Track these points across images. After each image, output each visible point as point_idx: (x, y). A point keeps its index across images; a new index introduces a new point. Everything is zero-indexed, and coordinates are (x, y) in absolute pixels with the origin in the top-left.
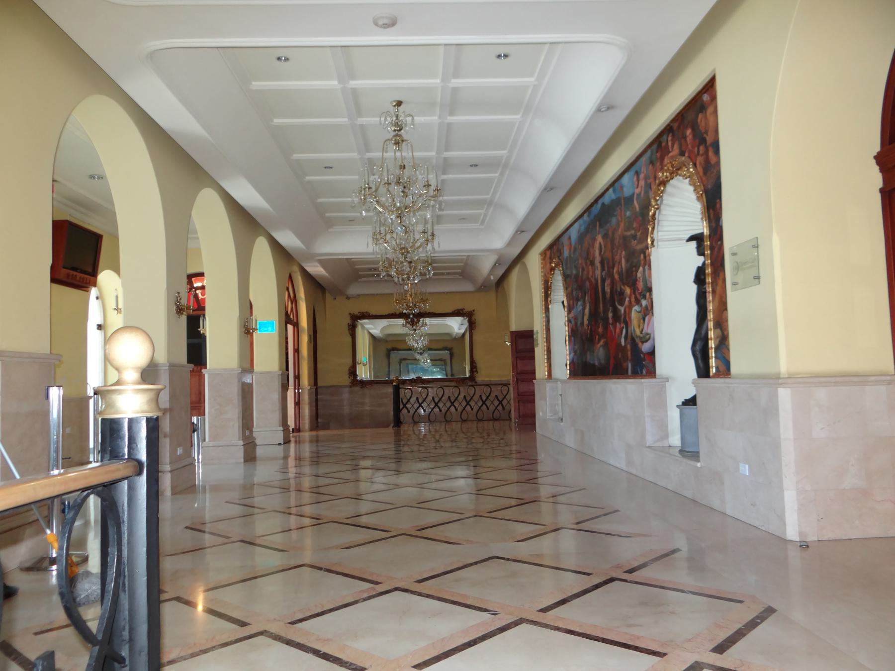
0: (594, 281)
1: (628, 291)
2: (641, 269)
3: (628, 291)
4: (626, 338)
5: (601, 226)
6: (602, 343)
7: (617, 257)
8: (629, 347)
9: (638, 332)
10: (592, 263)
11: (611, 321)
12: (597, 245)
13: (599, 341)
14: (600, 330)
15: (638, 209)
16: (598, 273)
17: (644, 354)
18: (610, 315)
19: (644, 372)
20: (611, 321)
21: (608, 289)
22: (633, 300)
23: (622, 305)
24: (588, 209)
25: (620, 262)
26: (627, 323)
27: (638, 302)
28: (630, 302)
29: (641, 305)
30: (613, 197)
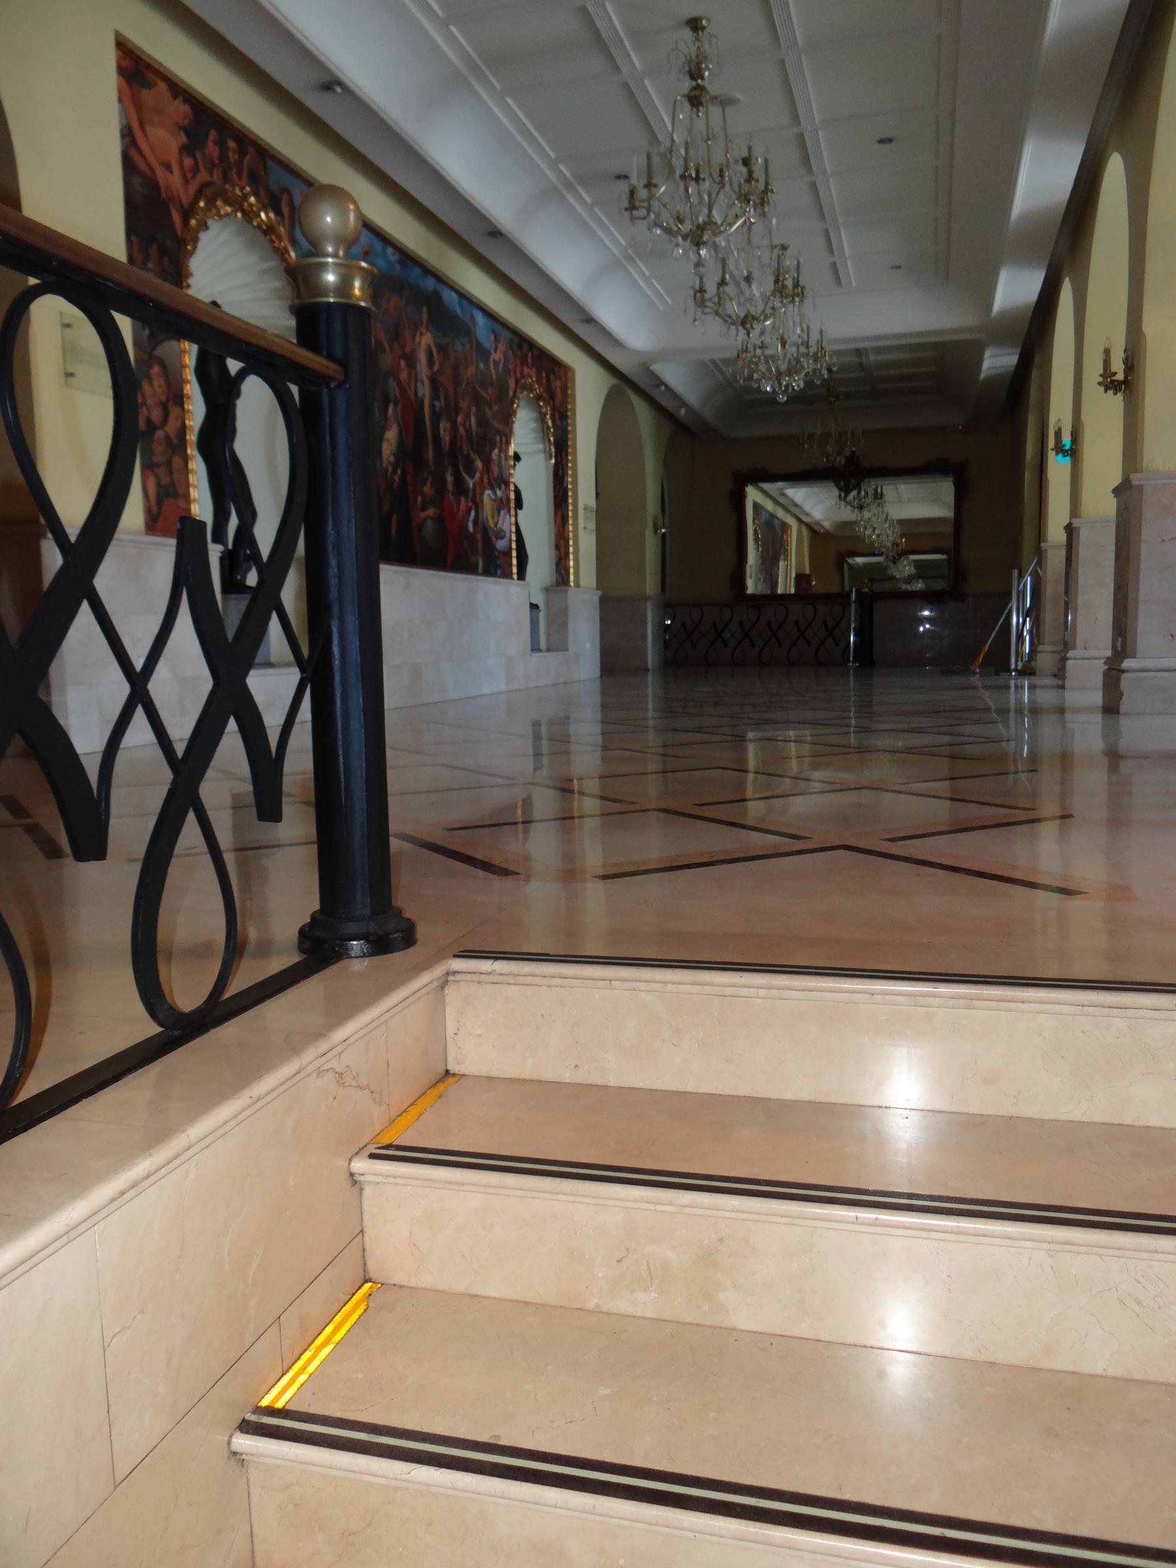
0: (413, 398)
1: (479, 464)
2: (496, 451)
3: (479, 464)
4: (476, 522)
5: (431, 320)
6: (430, 512)
7: (464, 404)
8: (479, 537)
9: (491, 523)
10: (411, 361)
11: (450, 487)
12: (423, 346)
13: (424, 508)
14: (428, 489)
15: (494, 377)
16: (424, 390)
17: (499, 552)
18: (449, 478)
19: (499, 572)
20: (450, 487)
21: (446, 438)
22: (486, 480)
23: (472, 476)
24: (407, 257)
25: (468, 416)
26: (478, 506)
27: (492, 488)
28: (481, 479)
29: (495, 494)
30: (458, 309)
